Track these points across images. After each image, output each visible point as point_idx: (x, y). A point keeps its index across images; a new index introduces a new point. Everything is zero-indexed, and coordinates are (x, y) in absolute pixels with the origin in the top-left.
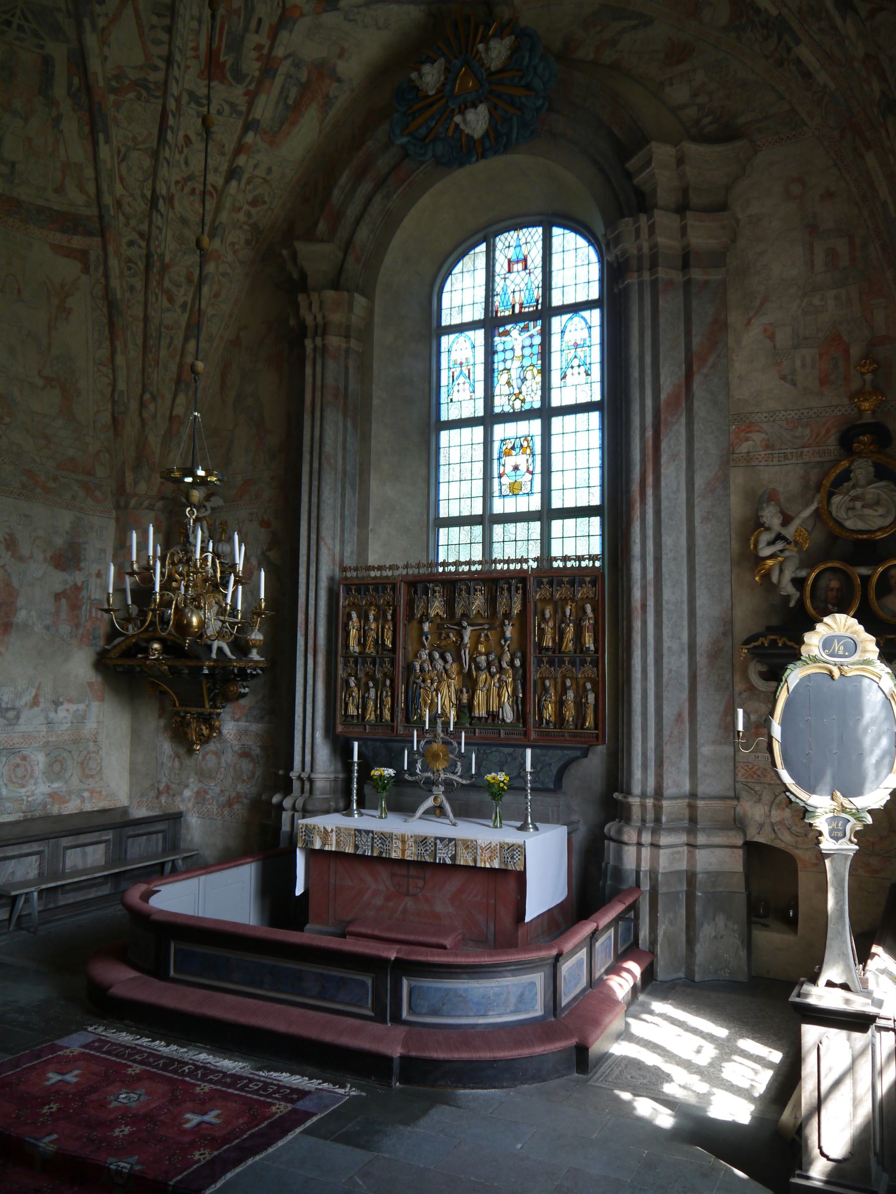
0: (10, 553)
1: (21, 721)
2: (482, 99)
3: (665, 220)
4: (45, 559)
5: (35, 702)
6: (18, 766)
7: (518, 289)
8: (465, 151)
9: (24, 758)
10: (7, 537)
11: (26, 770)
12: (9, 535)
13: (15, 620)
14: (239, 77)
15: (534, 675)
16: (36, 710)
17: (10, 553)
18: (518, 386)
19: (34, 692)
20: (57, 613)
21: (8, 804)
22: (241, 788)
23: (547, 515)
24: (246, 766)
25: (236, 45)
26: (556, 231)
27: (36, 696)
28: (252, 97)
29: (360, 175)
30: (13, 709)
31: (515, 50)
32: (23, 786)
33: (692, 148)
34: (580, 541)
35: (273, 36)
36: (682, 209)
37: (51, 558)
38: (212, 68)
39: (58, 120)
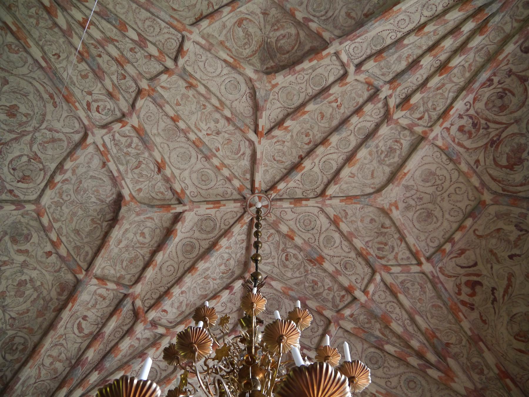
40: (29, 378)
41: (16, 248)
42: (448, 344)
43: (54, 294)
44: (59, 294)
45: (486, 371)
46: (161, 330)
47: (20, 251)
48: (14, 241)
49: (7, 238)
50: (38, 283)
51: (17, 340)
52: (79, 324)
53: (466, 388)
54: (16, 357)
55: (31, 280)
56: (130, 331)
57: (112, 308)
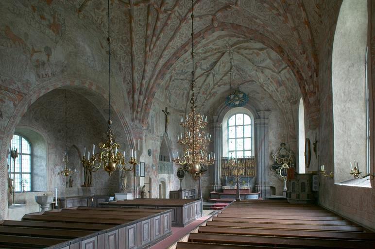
2: (234, 98)
3: (262, 119)
7: (239, 122)
8: (235, 106)
14: (206, 94)
15: (247, 170)
18: (240, 135)
22: (205, 185)
23: (244, 151)
24: (205, 183)
25: (207, 91)
26: (245, 115)
28: (207, 97)
29: (221, 107)
31: (243, 96)
33: (266, 112)
34: (248, 155)
35: (212, 90)
36: (264, 118)
38: (203, 93)
39: (183, 99)
40: (136, 49)
41: (101, 10)
42: (289, 5)
43: (124, 17)
44: (126, 16)
45: (301, 18)
46: (169, 12)
47: (103, 11)
48: (98, 9)
49: (96, 10)
50: (116, 16)
51: (124, 38)
52: (140, 24)
53: (291, 27)
54: (127, 44)
55: (114, 17)
56: (158, 19)
57: (147, 11)
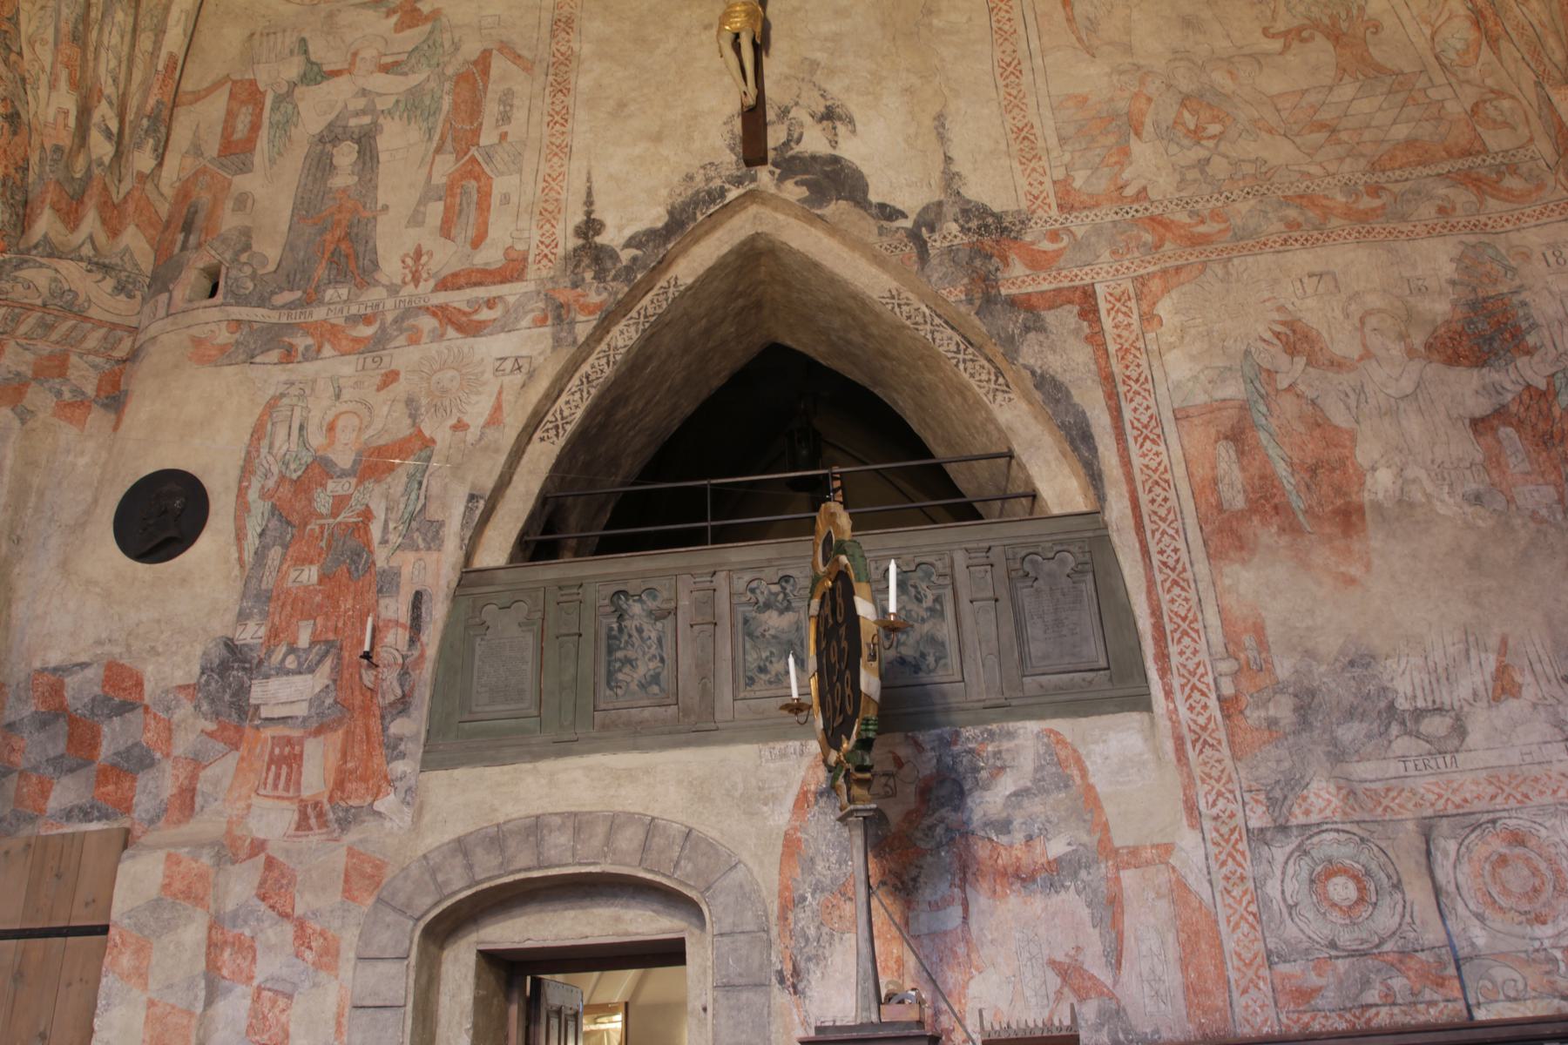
0: (1300, 361)
1: (1475, 737)
4: (1411, 353)
5: (1504, 686)
6: (1503, 860)
9: (1517, 839)
10: (1279, 328)
11: (1535, 872)
12: (1284, 323)
13: (1366, 497)
16: (1512, 707)
17: (1300, 361)
19: (1491, 663)
20: (1494, 461)
21: (1500, 973)
27: (1502, 671)
30: (1439, 710)
32: (1541, 920)
37: (1429, 346)
